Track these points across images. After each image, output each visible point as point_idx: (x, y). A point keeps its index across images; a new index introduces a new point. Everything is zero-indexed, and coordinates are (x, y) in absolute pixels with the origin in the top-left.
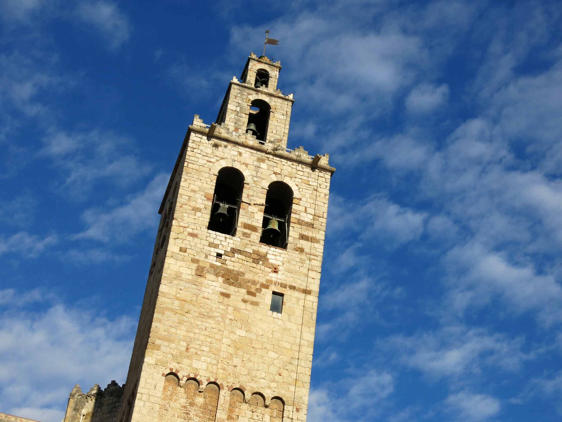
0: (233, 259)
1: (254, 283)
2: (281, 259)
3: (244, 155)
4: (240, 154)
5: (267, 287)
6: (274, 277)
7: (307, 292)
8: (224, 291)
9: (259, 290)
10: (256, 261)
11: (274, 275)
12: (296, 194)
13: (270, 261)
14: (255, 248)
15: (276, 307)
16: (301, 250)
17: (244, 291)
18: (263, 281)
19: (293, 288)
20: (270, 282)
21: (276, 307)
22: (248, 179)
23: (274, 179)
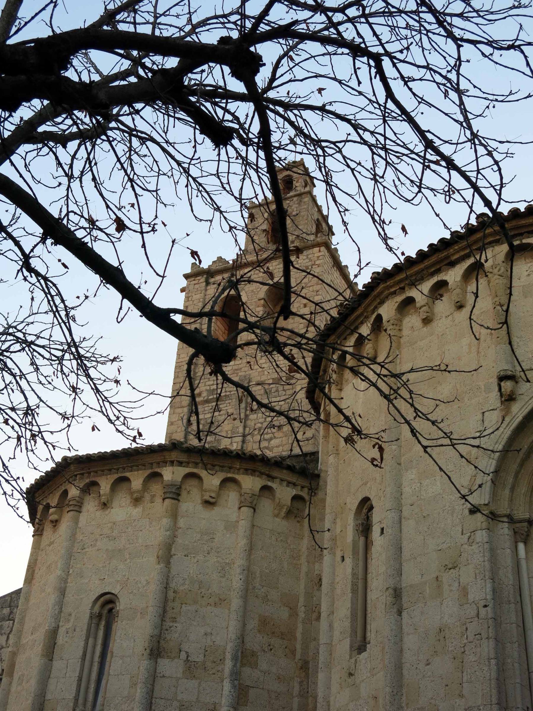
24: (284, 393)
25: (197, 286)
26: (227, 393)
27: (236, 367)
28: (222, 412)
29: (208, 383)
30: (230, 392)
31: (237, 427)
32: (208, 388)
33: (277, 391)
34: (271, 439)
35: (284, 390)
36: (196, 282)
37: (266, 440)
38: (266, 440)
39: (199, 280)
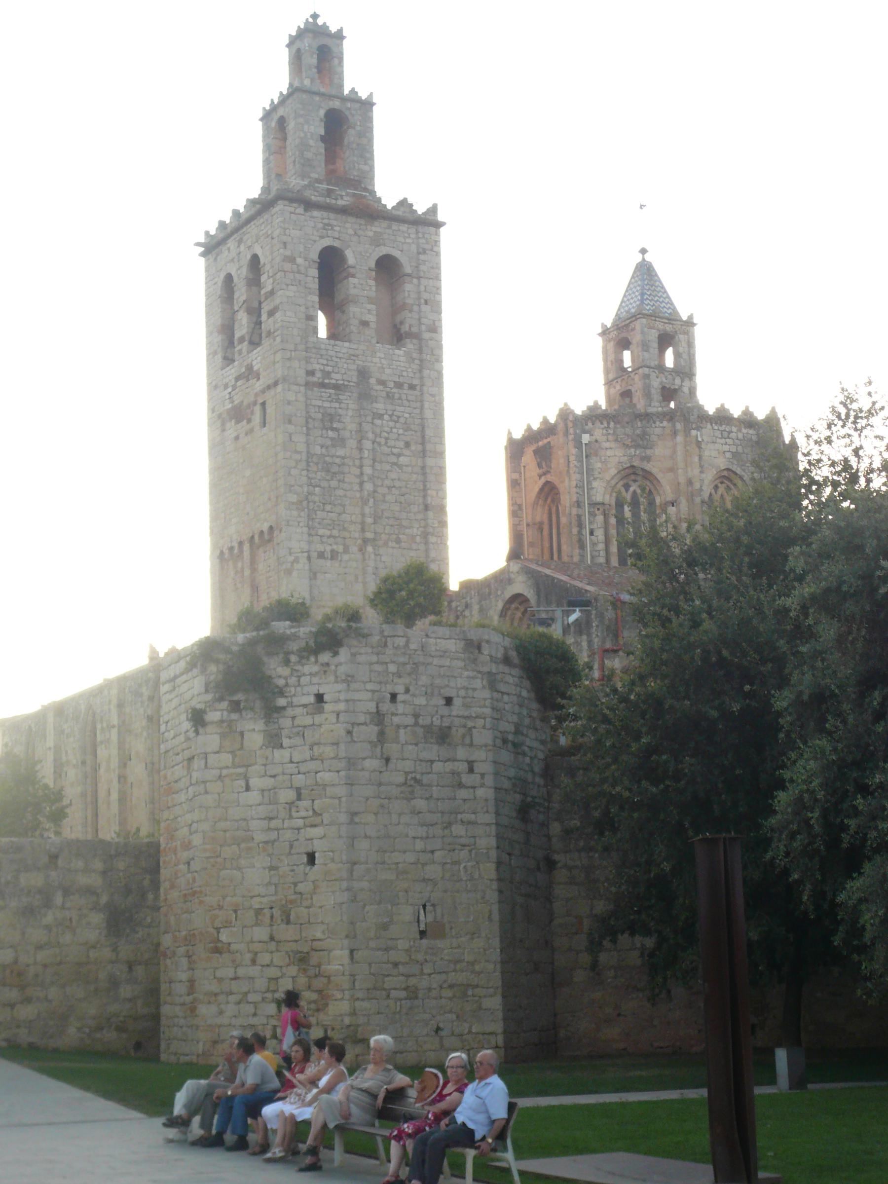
0: (237, 390)
1: (249, 406)
2: (259, 358)
3: (232, 248)
4: (229, 249)
5: (255, 403)
6: (258, 386)
7: (276, 384)
8: (235, 434)
9: (252, 413)
10: (248, 380)
11: (258, 384)
12: (262, 263)
13: (255, 368)
14: (245, 364)
15: (264, 424)
16: (269, 333)
17: (245, 421)
18: (252, 399)
19: (269, 387)
20: (256, 395)
21: (264, 424)
22: (235, 279)
23: (249, 257)
24: (407, 404)
25: (294, 217)
26: (346, 383)
27: (351, 352)
28: (343, 405)
29: (321, 361)
30: (349, 382)
31: (367, 432)
32: (322, 368)
33: (400, 398)
34: (399, 455)
35: (408, 401)
36: (292, 209)
37: (394, 454)
38: (394, 454)
39: (296, 208)
